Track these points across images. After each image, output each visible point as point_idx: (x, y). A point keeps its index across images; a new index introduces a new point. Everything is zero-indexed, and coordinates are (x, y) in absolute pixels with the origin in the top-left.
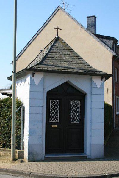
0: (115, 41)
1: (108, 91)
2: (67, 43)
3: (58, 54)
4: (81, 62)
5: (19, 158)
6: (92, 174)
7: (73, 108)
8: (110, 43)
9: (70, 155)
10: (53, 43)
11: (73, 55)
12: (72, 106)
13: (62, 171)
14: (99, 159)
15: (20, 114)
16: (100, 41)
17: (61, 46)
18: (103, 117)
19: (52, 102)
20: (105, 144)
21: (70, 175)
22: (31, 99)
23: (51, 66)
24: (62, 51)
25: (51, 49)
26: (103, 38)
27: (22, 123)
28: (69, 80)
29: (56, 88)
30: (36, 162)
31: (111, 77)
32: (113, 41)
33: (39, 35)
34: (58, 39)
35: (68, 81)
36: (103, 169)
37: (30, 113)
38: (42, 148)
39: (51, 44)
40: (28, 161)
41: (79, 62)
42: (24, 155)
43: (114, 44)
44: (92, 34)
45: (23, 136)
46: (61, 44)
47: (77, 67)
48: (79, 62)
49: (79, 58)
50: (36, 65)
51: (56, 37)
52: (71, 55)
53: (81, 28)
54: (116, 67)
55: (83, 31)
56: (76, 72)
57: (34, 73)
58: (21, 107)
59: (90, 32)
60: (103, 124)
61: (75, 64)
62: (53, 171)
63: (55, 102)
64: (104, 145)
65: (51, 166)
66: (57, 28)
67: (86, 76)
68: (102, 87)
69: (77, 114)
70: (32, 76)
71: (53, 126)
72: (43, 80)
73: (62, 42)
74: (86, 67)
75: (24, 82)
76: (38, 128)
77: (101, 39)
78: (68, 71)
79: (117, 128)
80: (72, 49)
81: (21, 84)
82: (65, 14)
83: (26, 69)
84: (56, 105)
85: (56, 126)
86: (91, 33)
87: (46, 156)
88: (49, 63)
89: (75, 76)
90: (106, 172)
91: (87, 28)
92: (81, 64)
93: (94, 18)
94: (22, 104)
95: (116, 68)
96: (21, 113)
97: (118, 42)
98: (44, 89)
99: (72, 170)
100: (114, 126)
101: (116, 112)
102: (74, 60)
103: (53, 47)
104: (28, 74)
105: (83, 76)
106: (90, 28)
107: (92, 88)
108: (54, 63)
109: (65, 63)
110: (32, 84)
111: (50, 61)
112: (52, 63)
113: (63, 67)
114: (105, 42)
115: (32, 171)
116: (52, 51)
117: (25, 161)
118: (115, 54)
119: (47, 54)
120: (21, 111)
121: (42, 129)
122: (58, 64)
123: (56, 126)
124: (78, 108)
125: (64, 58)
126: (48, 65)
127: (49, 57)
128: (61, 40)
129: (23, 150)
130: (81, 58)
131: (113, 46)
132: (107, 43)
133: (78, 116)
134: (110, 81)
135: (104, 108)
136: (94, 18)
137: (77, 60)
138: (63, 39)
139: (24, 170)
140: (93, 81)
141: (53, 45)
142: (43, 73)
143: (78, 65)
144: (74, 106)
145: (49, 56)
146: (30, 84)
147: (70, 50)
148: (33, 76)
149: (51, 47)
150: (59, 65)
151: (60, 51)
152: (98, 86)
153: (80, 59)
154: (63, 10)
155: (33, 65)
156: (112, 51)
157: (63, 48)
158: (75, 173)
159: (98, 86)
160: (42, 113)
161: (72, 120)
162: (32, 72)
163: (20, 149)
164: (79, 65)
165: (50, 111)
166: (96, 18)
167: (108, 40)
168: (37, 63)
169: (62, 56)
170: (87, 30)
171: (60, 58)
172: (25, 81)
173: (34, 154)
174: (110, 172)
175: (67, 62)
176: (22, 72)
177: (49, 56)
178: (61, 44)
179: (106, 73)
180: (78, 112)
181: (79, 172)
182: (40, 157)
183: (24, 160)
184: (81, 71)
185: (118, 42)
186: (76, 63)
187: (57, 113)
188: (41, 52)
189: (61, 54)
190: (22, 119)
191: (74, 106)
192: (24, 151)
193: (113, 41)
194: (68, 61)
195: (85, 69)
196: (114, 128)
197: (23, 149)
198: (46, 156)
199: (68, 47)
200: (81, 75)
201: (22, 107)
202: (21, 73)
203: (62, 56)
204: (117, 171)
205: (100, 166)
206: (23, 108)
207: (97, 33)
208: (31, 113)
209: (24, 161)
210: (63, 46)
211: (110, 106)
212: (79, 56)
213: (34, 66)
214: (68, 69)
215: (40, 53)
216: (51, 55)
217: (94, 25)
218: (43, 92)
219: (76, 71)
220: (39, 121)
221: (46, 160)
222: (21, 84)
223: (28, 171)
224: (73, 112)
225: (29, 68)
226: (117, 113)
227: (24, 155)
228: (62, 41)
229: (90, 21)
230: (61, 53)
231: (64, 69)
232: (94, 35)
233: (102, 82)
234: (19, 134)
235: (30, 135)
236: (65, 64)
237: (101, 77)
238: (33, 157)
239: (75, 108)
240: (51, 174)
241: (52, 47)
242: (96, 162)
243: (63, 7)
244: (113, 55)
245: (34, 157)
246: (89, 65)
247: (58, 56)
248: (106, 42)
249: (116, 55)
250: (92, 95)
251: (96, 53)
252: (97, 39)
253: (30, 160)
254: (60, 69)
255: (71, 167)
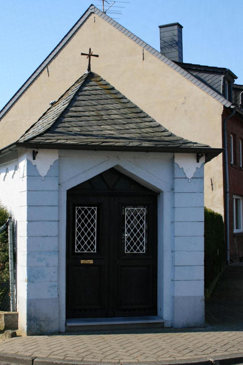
0: (229, 76)
1: (212, 184)
2: (113, 84)
3: (93, 109)
4: (147, 123)
5: (6, 328)
6: (177, 358)
7: (129, 222)
8: (217, 81)
9: (123, 320)
10: (78, 86)
11: (126, 110)
12: (127, 218)
13: (108, 353)
14: (194, 327)
15: (7, 237)
16: (192, 77)
17: (98, 92)
18: (202, 239)
19: (80, 212)
20: (208, 296)
21: (124, 361)
22: (30, 206)
23: (75, 134)
24: (102, 102)
25: (73, 100)
26: (200, 71)
27: (10, 256)
28: (120, 164)
29: (89, 181)
30: (46, 337)
31: (221, 155)
32: (223, 76)
33: (46, 69)
34: (90, 77)
35: (118, 166)
36: (203, 348)
37: (29, 236)
38: (59, 306)
39: (75, 89)
40: (28, 335)
41: (142, 125)
42: (17, 322)
43: (226, 82)
44: (173, 63)
45: (15, 283)
46: (98, 87)
47: (138, 135)
48: (142, 125)
49: (142, 115)
50: (40, 135)
51: (87, 72)
52: (122, 111)
53: (145, 51)
54: (232, 133)
55: (150, 57)
56: (137, 147)
57: (37, 152)
58: (7, 225)
59: (166, 59)
60: (203, 254)
61: (133, 130)
62: (84, 354)
63: (86, 212)
64: (204, 297)
65: (80, 344)
66: (88, 53)
67: (158, 155)
68: (199, 177)
69: (138, 235)
70: (31, 158)
71: (82, 262)
72: (58, 165)
73: (102, 82)
74: (160, 134)
75: (13, 171)
76: (48, 265)
77: (195, 74)
78: (117, 144)
79: (237, 263)
80: (124, 98)
81: (6, 176)
82: (105, 23)
83: (17, 144)
84: (89, 217)
85: (91, 262)
86: (170, 61)
87: (68, 324)
88: (70, 129)
89: (136, 154)
90: (211, 355)
91: (159, 50)
92: (148, 130)
93: (176, 27)
94: (11, 218)
95: (231, 136)
96: (7, 236)
97: (236, 78)
98: (59, 184)
99: (131, 352)
100: (229, 259)
101: (232, 228)
102: (129, 121)
103: (80, 94)
104: (21, 154)
105: (152, 154)
106: (167, 50)
107: (174, 178)
108: (83, 128)
109: (108, 127)
110: (32, 174)
111: (69, 124)
112: (77, 129)
113: (104, 136)
114: (206, 80)
115: (37, 355)
116: (76, 103)
117: (22, 334)
118: (228, 105)
119: (66, 110)
120: (7, 233)
121: (59, 267)
122: (92, 130)
123: (91, 262)
124: (141, 222)
125: (105, 117)
126: (69, 133)
127: (71, 117)
128: (98, 79)
129: (14, 313)
130: (147, 116)
131: (224, 87)
132: (208, 82)
133: (141, 239)
134: (217, 163)
135: (203, 220)
136: (176, 27)
137: (138, 120)
138: (103, 77)
139: (19, 353)
140: (175, 166)
141: (80, 90)
142: (58, 150)
143: (138, 131)
144: (132, 218)
145: (70, 114)
146: (28, 176)
147: (120, 98)
148: (34, 158)
149: (75, 95)
150: (95, 133)
151: (96, 104)
152: (190, 175)
153: (144, 119)
154: (101, 13)
155: (35, 135)
156: (222, 99)
157: (103, 97)
158: (137, 358)
159: (190, 175)
160: (56, 233)
161: (129, 248)
162: (31, 150)
163: (9, 310)
164: (143, 130)
165: (75, 229)
166: (180, 27)
167: (211, 76)
168: (42, 130)
169: (102, 113)
170: (160, 55)
171: (98, 118)
172: (16, 168)
173: (40, 321)
174: (219, 354)
175: (113, 126)
176: (8, 151)
177: (70, 114)
178: (98, 87)
179: (208, 146)
180: (141, 231)
181: (146, 355)
182: (54, 327)
183: (18, 332)
184: (146, 144)
185: (236, 78)
186: (134, 127)
187: (92, 234)
188: (51, 106)
189: (100, 109)
190: (10, 248)
191: (132, 218)
192: (18, 314)
193: (223, 76)
194: (115, 124)
195: (155, 138)
196: (227, 262)
197: (15, 310)
198: (68, 324)
199: (116, 94)
200: (147, 152)
201: (11, 224)
202: (6, 152)
203: (102, 113)
204: (236, 352)
205: (196, 342)
206: (13, 225)
207: (185, 61)
208: (30, 237)
209: (18, 334)
210: (103, 91)
211: (219, 216)
212: (141, 112)
213: (35, 137)
214: (117, 140)
215: (50, 108)
216: (76, 112)
217: (177, 44)
218: (59, 191)
219: (136, 144)
220: (50, 252)
221: (69, 331)
222: (6, 176)
223: (28, 354)
224: (129, 230)
225: (25, 141)
226: (235, 231)
227: (17, 322)
228: (102, 80)
229: (166, 34)
230: (100, 107)
231: (106, 140)
232: (176, 66)
233: (199, 165)
234: (5, 280)
235: (31, 280)
236: (108, 130)
237: (196, 154)
238: (38, 327)
239: (135, 222)
240: (82, 360)
241: (77, 94)
242: (186, 334)
243: (101, 8)
244: (224, 107)
245: (40, 326)
246: (165, 131)
247: (93, 113)
248: (208, 78)
249: (232, 107)
250: (174, 193)
251: (183, 104)
252: (186, 72)
253: (31, 332)
254: (97, 140)
255: (126, 346)
